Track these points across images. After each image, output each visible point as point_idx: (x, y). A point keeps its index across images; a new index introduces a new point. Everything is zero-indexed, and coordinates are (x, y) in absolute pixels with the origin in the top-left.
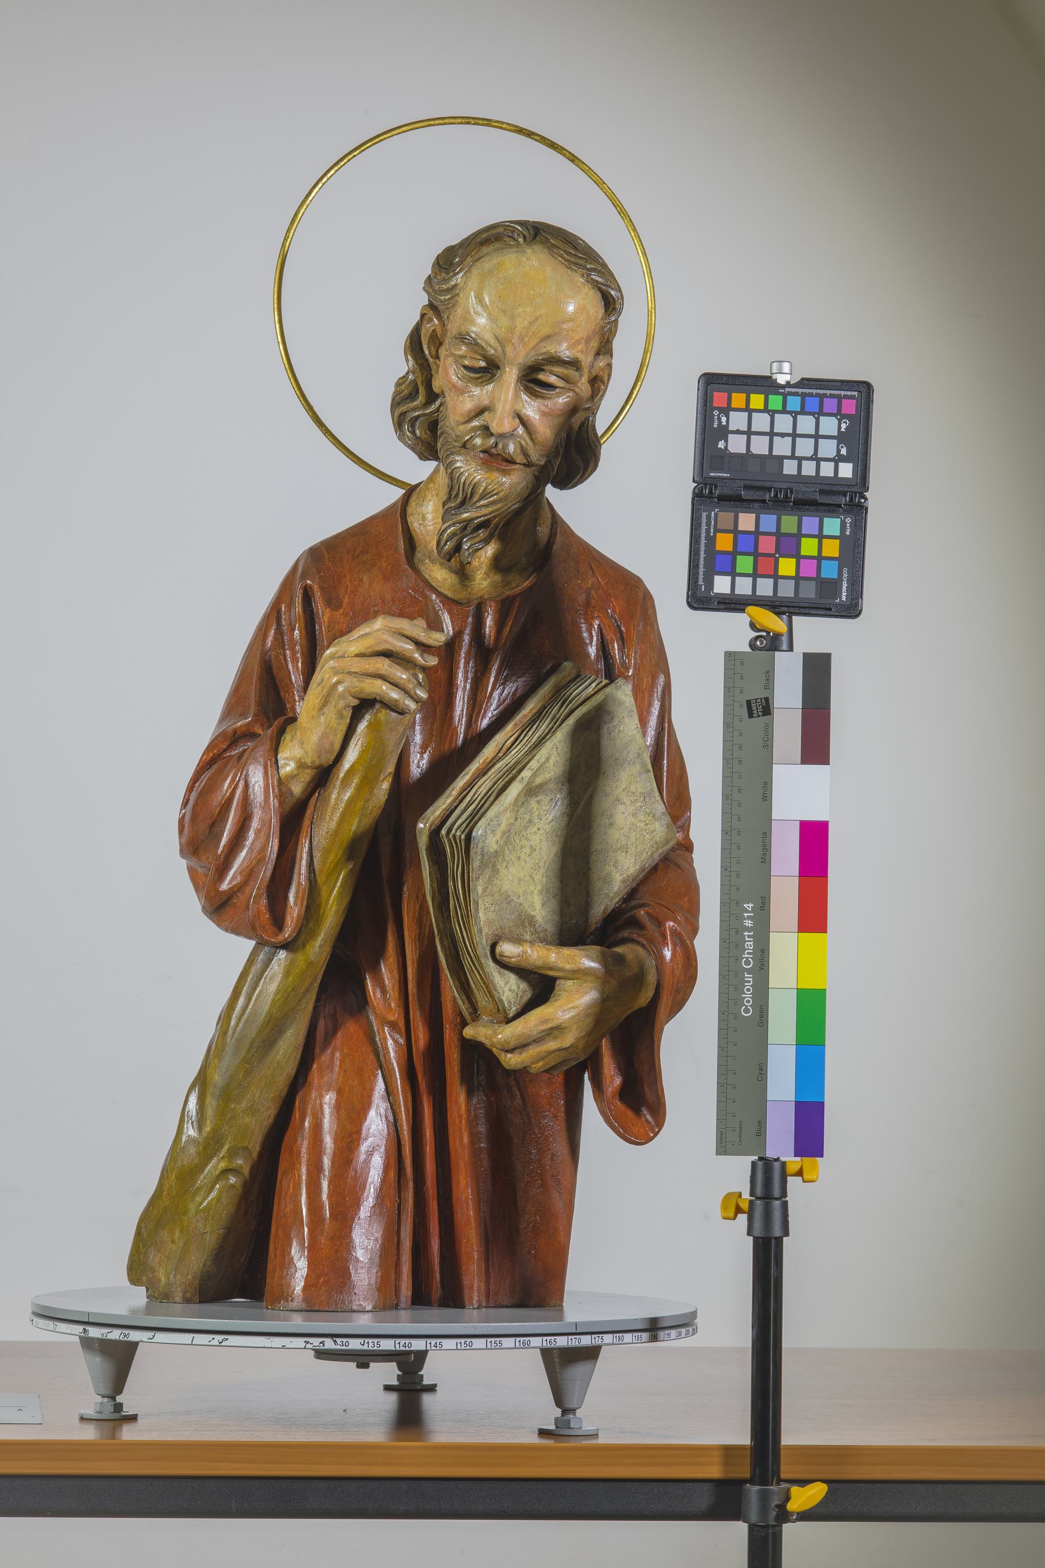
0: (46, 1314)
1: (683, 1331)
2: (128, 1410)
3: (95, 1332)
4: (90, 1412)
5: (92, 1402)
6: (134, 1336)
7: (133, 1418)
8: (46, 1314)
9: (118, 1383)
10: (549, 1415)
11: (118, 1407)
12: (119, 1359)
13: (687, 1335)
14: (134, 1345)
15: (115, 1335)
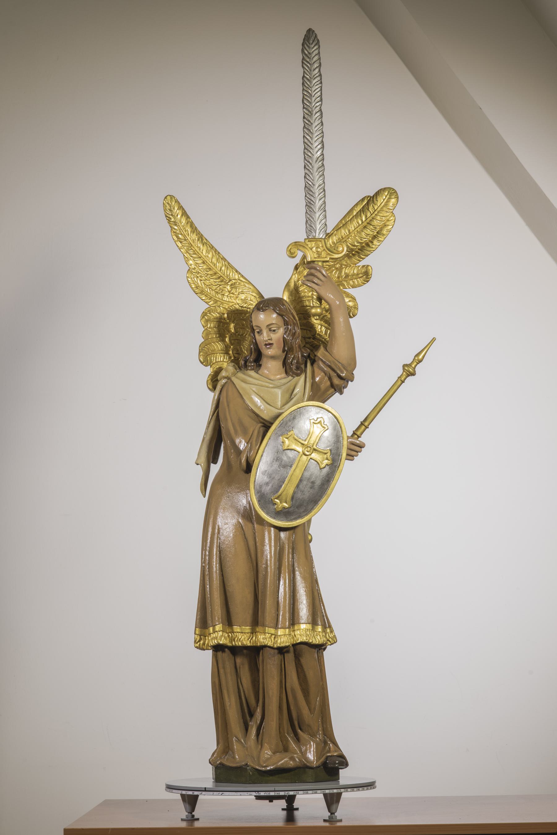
0: (170, 788)
1: (369, 787)
2: (196, 817)
3: (184, 792)
4: (184, 817)
5: (184, 814)
6: (196, 793)
7: (198, 819)
8: (170, 788)
9: (193, 810)
10: (327, 814)
11: (193, 816)
12: (191, 801)
13: (371, 789)
14: (197, 796)
15: (190, 793)
